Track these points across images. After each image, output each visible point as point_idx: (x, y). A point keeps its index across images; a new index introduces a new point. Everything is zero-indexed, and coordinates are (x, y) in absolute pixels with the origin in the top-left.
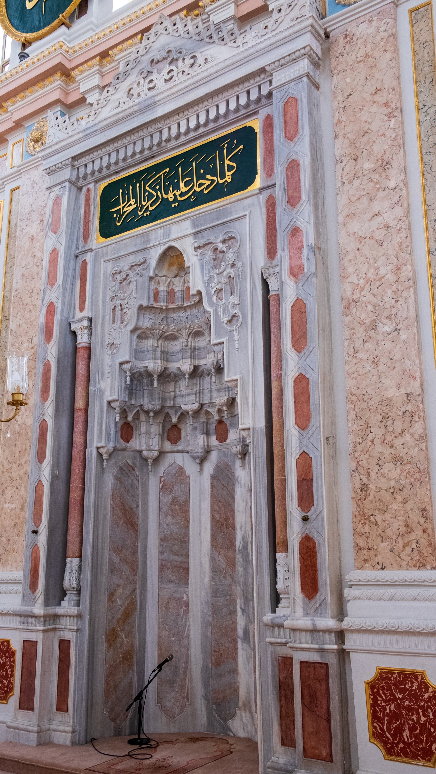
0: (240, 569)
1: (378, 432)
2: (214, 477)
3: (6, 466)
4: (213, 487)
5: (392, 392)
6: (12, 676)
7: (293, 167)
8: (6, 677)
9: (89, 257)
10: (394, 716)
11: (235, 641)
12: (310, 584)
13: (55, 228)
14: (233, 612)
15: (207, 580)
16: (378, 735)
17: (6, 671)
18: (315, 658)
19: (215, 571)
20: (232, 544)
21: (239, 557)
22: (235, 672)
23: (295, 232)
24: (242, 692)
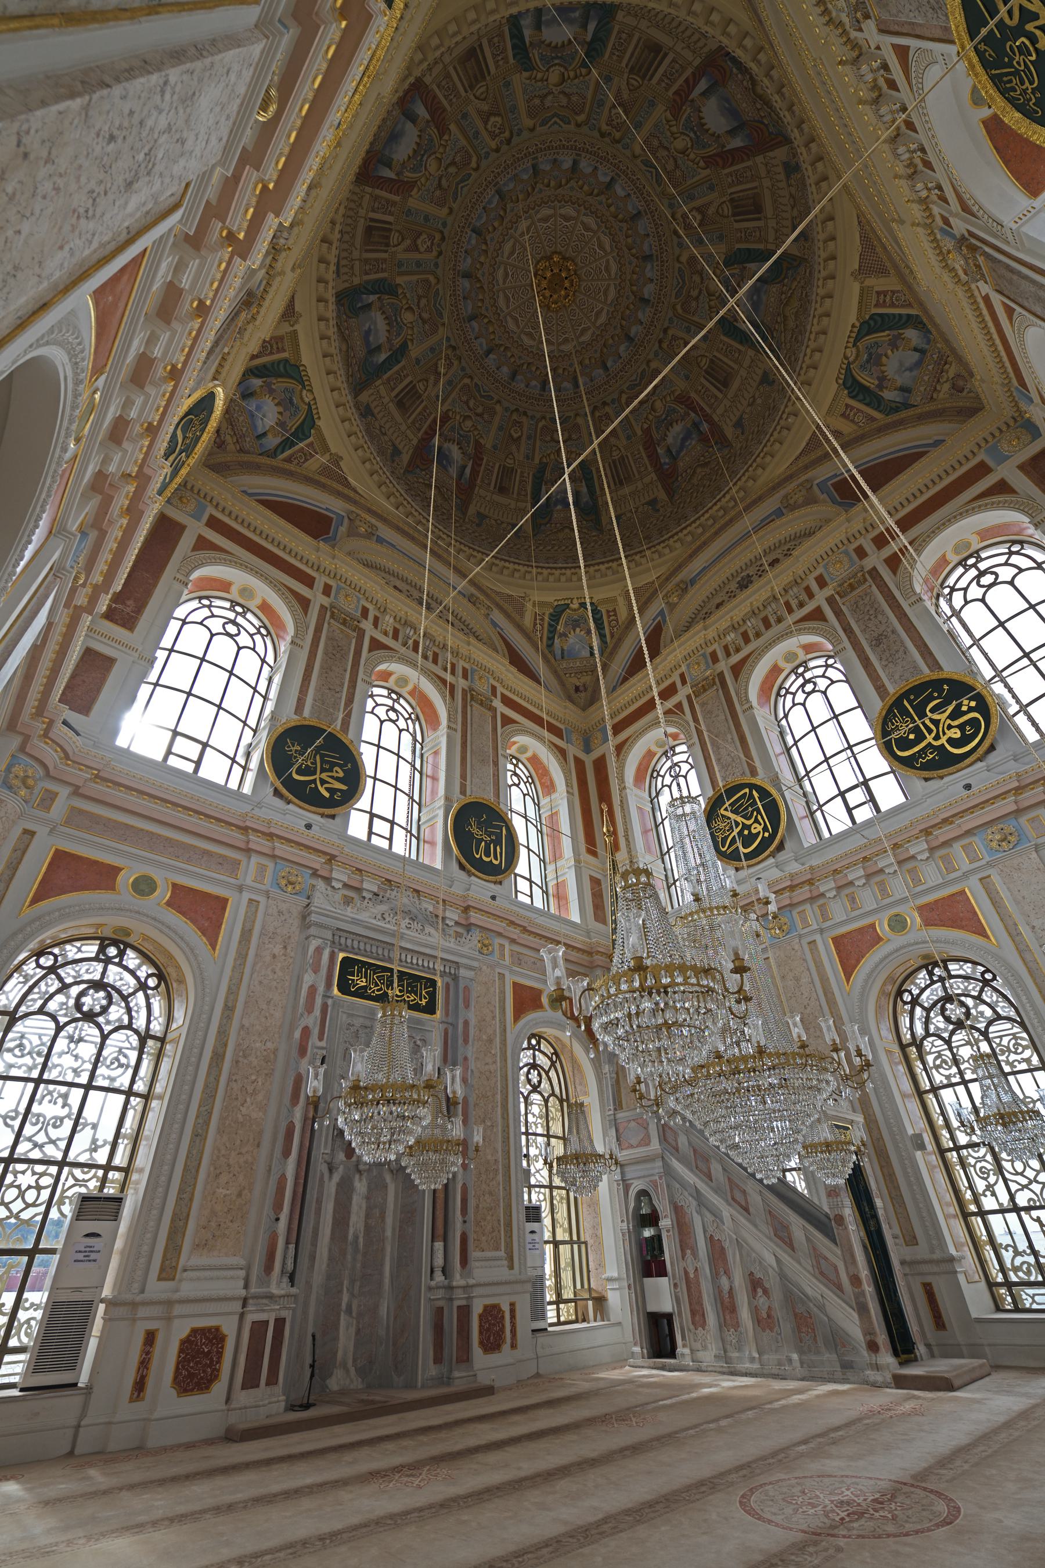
0: (349, 1257)
1: (484, 1177)
2: (338, 1185)
3: (223, 1152)
4: (337, 1193)
5: (489, 1157)
6: (219, 1362)
7: (466, 1023)
8: (210, 1366)
9: (330, 1002)
10: (488, 1330)
11: (339, 1315)
12: (464, 1261)
13: (316, 971)
14: (341, 1292)
15: (324, 1266)
16: (481, 1343)
17: (211, 1360)
18: (464, 1303)
19: (331, 1258)
20: (346, 1237)
21: (350, 1249)
22: (336, 1339)
23: (466, 1059)
24: (340, 1354)
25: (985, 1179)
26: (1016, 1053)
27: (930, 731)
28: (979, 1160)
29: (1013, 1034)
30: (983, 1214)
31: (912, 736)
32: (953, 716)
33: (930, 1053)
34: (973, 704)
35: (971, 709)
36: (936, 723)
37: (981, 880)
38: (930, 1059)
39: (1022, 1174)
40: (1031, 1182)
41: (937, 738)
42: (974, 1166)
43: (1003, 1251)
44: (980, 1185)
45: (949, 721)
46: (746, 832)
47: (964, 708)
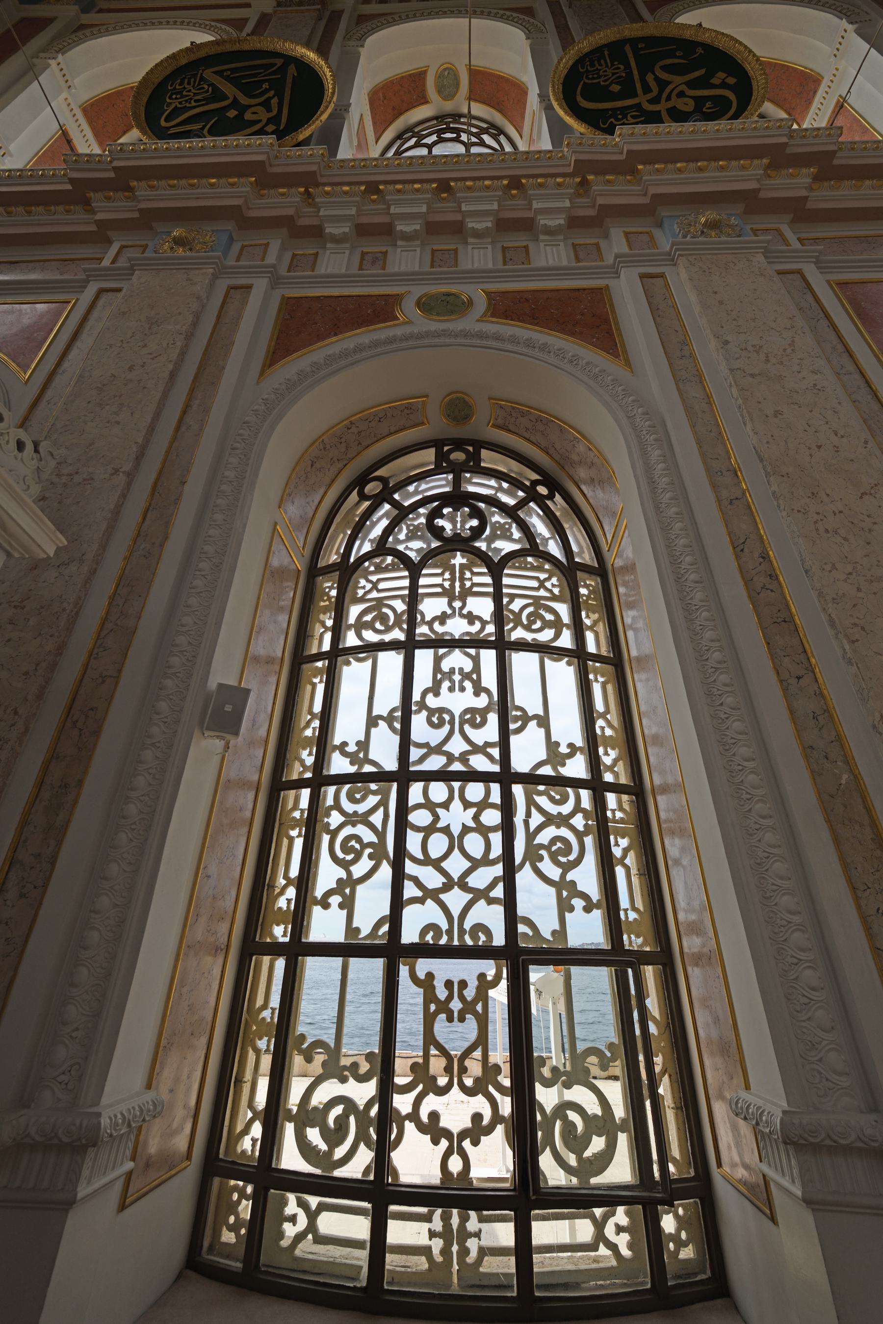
25: (345, 865)
26: (528, 628)
27: (647, 89)
28: (352, 819)
29: (537, 599)
30: (298, 950)
31: (616, 88)
32: (691, 84)
33: (362, 600)
34: (731, 81)
35: (724, 85)
36: (662, 84)
37: (642, 276)
38: (354, 612)
39: (436, 864)
40: (447, 887)
41: (655, 101)
42: (334, 834)
43: (298, 1060)
44: (328, 874)
45: (684, 87)
46: (232, 113)
47: (715, 81)
